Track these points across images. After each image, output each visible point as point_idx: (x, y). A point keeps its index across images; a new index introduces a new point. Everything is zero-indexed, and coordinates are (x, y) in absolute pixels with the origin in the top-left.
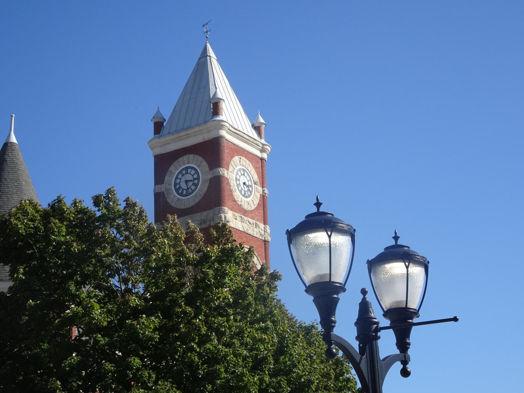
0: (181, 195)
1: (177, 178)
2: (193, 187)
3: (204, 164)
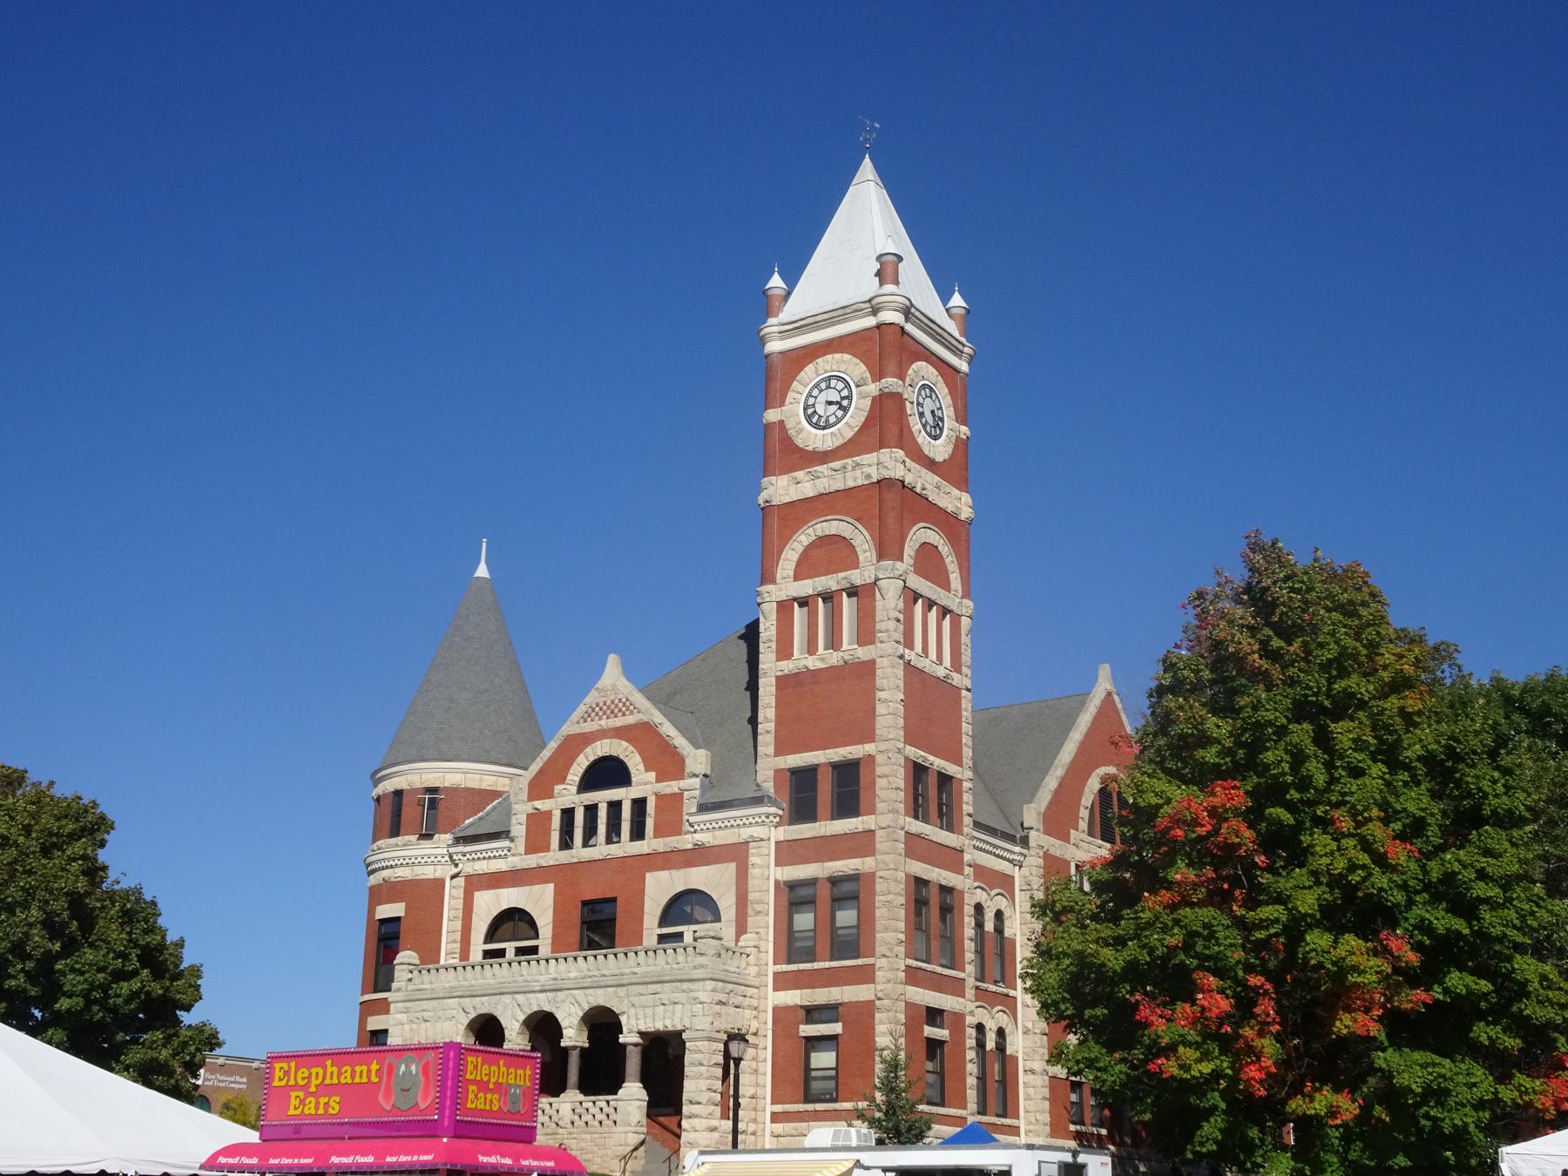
0: (817, 426)
1: (810, 395)
2: (839, 413)
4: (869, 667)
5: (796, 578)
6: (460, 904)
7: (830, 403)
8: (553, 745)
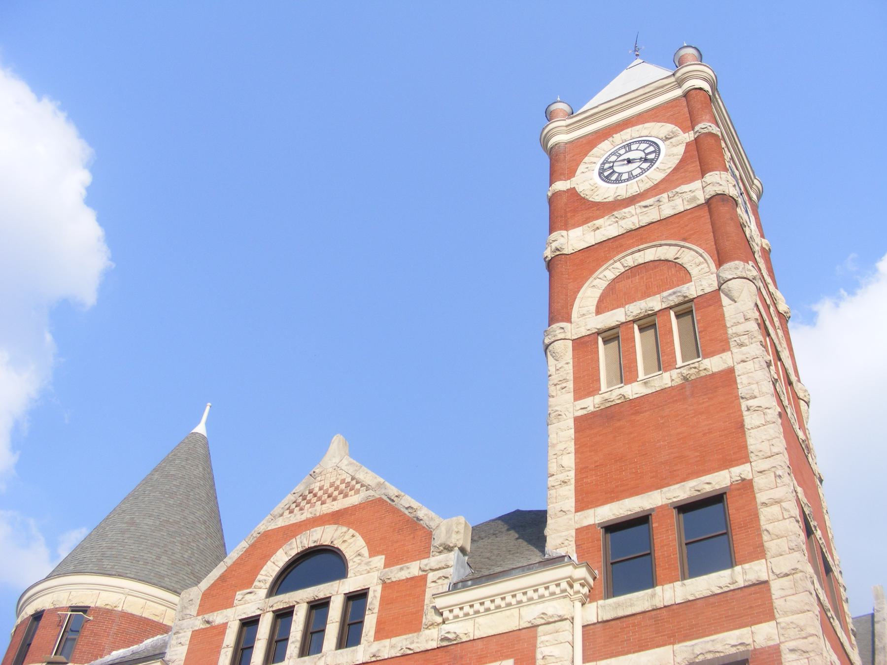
4: (728, 376)
5: (600, 309)
8: (244, 545)
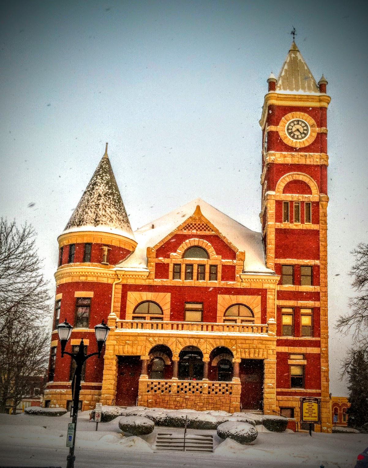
3: (313, 121)
5: (284, 192)
6: (120, 296)
7: (298, 130)
